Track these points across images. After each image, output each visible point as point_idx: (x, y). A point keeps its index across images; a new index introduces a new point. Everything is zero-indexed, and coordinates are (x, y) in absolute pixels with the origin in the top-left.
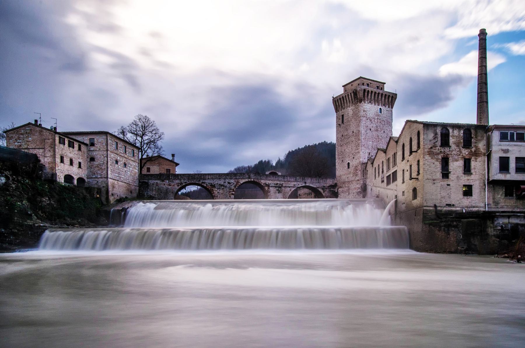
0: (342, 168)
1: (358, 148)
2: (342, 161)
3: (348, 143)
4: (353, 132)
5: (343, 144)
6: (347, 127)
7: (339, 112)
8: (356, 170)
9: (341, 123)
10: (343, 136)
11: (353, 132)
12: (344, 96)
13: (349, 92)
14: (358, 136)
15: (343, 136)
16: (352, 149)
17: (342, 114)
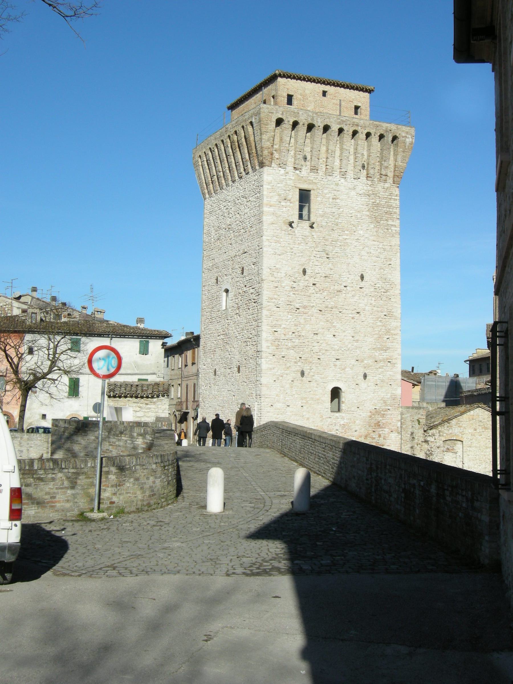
0: (300, 404)
1: (389, 345)
2: (303, 374)
3: (336, 311)
4: (362, 277)
5: (305, 307)
6: (329, 248)
7: (282, 171)
8: (378, 425)
9: (295, 218)
10: (304, 272)
11: (362, 277)
12: (335, 128)
13: (365, 127)
14: (384, 298)
15: (304, 272)
16: (357, 341)
17: (305, 187)
